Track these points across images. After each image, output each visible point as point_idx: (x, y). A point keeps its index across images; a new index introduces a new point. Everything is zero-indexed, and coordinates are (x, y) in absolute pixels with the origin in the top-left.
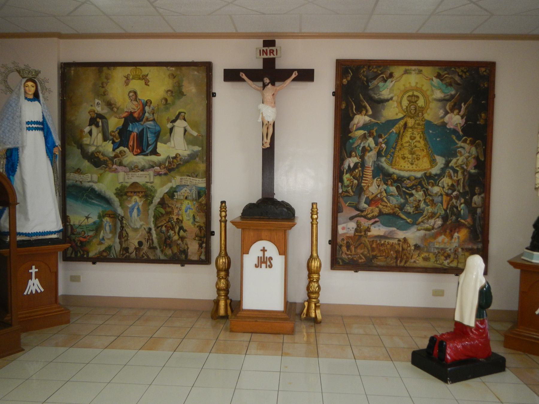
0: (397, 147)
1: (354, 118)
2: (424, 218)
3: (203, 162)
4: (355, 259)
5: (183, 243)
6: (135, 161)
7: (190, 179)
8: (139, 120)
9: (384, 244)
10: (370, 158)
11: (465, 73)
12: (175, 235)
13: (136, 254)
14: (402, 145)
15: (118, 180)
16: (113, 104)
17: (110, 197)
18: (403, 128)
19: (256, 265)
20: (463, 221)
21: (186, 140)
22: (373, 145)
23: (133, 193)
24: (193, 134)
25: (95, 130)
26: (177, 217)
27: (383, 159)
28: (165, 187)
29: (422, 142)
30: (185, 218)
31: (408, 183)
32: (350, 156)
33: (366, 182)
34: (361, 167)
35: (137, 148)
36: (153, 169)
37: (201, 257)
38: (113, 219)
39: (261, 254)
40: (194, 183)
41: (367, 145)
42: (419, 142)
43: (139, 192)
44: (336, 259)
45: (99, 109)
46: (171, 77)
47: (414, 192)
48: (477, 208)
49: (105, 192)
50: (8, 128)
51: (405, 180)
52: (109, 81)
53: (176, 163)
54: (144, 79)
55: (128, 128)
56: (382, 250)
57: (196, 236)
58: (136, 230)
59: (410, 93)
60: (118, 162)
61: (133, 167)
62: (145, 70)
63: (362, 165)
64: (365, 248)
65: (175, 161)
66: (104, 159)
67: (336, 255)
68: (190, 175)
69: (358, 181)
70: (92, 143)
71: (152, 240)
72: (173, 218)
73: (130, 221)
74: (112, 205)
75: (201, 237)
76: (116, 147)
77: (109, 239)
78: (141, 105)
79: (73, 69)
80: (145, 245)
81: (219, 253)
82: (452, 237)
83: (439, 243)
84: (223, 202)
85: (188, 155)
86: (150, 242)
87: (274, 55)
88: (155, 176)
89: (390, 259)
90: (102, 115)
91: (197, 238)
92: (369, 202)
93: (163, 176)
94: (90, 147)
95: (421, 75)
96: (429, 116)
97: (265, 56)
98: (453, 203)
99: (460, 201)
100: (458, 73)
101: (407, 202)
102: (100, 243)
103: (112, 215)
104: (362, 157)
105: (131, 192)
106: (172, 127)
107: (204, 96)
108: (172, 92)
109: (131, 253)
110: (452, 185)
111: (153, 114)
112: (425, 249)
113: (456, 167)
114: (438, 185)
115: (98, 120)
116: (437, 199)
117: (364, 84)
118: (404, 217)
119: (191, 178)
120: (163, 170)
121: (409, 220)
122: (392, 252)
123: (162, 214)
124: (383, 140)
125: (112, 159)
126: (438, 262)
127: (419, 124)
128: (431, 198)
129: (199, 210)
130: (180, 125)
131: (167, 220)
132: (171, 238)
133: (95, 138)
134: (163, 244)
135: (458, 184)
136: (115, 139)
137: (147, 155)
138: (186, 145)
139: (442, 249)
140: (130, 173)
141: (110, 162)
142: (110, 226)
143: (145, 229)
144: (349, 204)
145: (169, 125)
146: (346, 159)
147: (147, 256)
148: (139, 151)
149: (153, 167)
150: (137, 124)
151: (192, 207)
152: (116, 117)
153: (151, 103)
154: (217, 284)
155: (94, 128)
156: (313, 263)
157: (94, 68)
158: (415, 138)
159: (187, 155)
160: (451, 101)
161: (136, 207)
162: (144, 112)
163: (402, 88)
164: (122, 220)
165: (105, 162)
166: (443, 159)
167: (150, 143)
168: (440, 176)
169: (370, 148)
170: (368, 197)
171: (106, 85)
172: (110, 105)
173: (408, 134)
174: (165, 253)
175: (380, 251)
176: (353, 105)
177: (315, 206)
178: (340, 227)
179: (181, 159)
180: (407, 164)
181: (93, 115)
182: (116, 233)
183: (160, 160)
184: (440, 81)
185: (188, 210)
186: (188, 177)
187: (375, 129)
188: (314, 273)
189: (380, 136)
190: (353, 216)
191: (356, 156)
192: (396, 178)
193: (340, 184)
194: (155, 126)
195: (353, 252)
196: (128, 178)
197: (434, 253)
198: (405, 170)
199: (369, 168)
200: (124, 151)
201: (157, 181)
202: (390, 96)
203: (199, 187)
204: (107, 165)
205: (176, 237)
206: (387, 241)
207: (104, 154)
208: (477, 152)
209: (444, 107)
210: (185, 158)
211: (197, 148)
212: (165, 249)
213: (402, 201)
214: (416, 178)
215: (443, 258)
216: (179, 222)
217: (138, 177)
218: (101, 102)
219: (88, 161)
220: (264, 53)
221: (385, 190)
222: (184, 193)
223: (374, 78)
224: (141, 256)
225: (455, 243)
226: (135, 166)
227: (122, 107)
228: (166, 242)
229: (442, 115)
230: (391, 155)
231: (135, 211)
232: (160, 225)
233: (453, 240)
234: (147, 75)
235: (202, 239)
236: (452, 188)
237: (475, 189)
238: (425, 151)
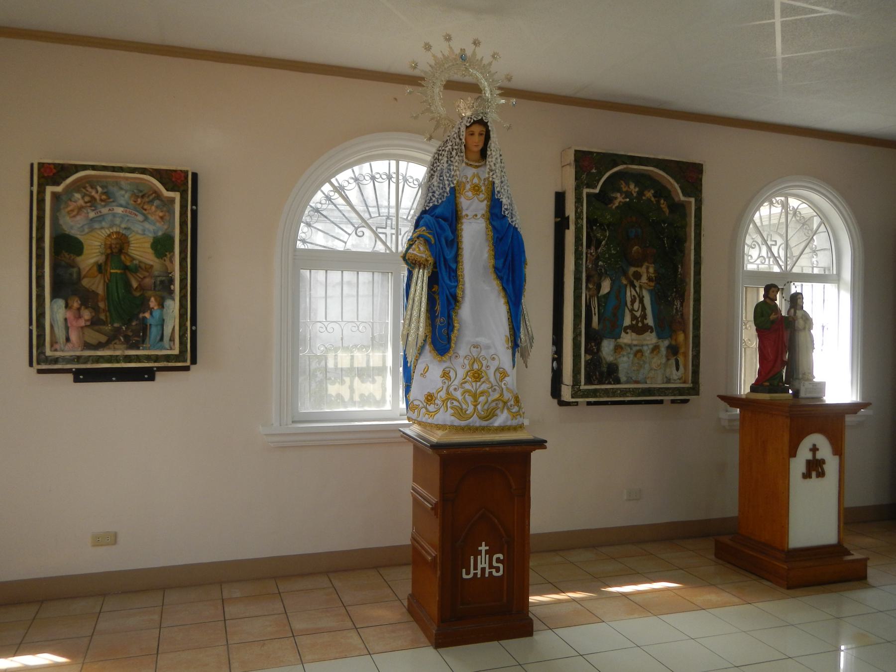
19: (803, 474)
39: (809, 456)
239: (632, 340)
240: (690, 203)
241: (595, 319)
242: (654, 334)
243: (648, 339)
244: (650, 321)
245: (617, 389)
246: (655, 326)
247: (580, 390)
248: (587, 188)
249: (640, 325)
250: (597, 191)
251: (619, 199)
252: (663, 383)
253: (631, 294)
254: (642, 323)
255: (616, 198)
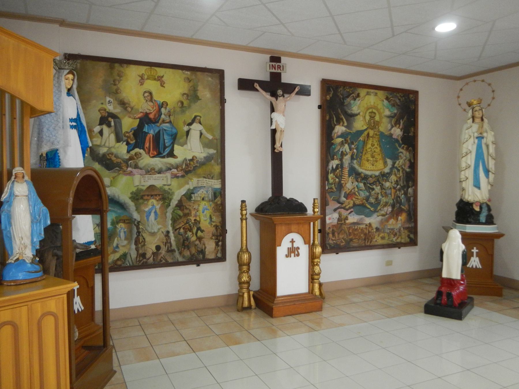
0: (364, 152)
1: (335, 128)
2: (381, 207)
3: (218, 164)
4: (338, 243)
5: (201, 243)
6: (151, 163)
7: (206, 181)
8: (155, 121)
9: (357, 229)
10: (347, 160)
11: (402, 97)
12: (193, 236)
13: (154, 259)
14: (366, 150)
15: (133, 183)
16: (127, 103)
17: (125, 201)
18: (366, 137)
19: (286, 255)
20: (403, 207)
21: (201, 143)
22: (348, 150)
23: (150, 196)
24: (209, 137)
25: (106, 130)
26: (195, 218)
27: (355, 161)
28: (182, 189)
29: (379, 148)
30: (203, 219)
31: (371, 180)
32: (333, 159)
33: (345, 180)
34: (340, 168)
35: (153, 150)
36: (170, 171)
37: (218, 255)
38: (128, 224)
39: (290, 245)
40: (210, 185)
41: (344, 150)
42: (377, 148)
43: (156, 195)
44: (326, 245)
45: (110, 108)
46: (186, 80)
47: (374, 187)
48: (410, 197)
49: (119, 197)
50: (53, 125)
51: (369, 178)
52: (121, 78)
53: (193, 166)
54: (159, 80)
55: (143, 130)
56: (356, 234)
57: (213, 235)
58: (153, 234)
59: (370, 110)
60: (134, 165)
61: (149, 169)
62: (161, 71)
63: (341, 166)
64: (345, 233)
65: (192, 163)
66: (118, 161)
67: (325, 242)
68: (206, 176)
69: (339, 179)
70: (103, 144)
71: (170, 243)
72: (191, 219)
73: (147, 225)
74: (127, 210)
75: (217, 236)
76: (131, 148)
77: (124, 246)
78: (157, 107)
79: (79, 61)
80: (163, 249)
81: (240, 249)
82: (397, 219)
83: (390, 225)
84: (243, 202)
85: (205, 157)
86: (168, 245)
87: (281, 70)
88: (172, 178)
89: (361, 241)
90: (114, 114)
91: (213, 237)
92: (347, 196)
93: (180, 178)
94: (101, 148)
95: (376, 96)
96: (382, 129)
97: (273, 71)
98: (397, 194)
99: (401, 192)
100: (398, 97)
101: (370, 195)
102: (114, 252)
103: (127, 220)
104: (341, 160)
105: (148, 195)
106: (188, 129)
107: (218, 101)
108: (188, 95)
109: (148, 259)
110: (397, 181)
111: (169, 116)
112: (382, 231)
113: (399, 167)
114: (389, 181)
115: (110, 119)
116: (388, 192)
117: (341, 100)
118: (369, 206)
119: (208, 180)
120: (180, 172)
121: (372, 209)
122: (362, 235)
123: (179, 216)
124: (355, 146)
125: (126, 161)
126: (390, 240)
127: (376, 135)
128: (385, 191)
129: (215, 210)
130: (196, 128)
131: (185, 222)
132: (189, 239)
133: (107, 139)
134: (181, 246)
135: (400, 180)
136: (129, 140)
137: (163, 157)
138: (202, 148)
139: (392, 229)
140: (147, 176)
141: (124, 164)
142: (125, 232)
143: (162, 232)
144: (333, 198)
145: (186, 128)
146: (330, 161)
147: (165, 260)
148: (155, 153)
149: (170, 169)
150: (153, 125)
151: (209, 208)
152: (130, 117)
153: (167, 105)
154: (239, 278)
155: (105, 128)
156: (317, 250)
157: (104, 63)
158: (374, 145)
159: (203, 158)
160: (394, 117)
161: (153, 211)
162: (160, 114)
163: (366, 106)
164: (139, 225)
165: (119, 165)
166: (391, 161)
167: (167, 145)
168: (390, 174)
169: (346, 152)
170: (345, 192)
171: (119, 83)
172: (123, 104)
173: (370, 142)
174: (183, 255)
175: (354, 234)
176: (334, 117)
177: (316, 201)
178: (327, 218)
179: (197, 162)
180: (370, 165)
181: (104, 114)
182: (131, 239)
183: (178, 163)
184: (388, 103)
185: (205, 210)
186: (205, 179)
187: (349, 138)
188: (244, 265)
189: (353, 143)
190: (336, 208)
191: (337, 159)
192: (363, 176)
193: (327, 182)
194: (172, 128)
195: (337, 238)
196: (144, 181)
197: (388, 233)
198: (368, 170)
199: (346, 168)
200: (139, 152)
201: (174, 183)
202: (358, 112)
203: (215, 188)
204: (121, 168)
205: (194, 238)
206: (359, 226)
207: (118, 156)
208: (410, 156)
209: (391, 122)
210: (201, 161)
211: (212, 151)
212: (183, 251)
213: (368, 194)
214: (376, 176)
215: (392, 236)
216: (196, 223)
217: (155, 179)
218: (113, 100)
219: (99, 163)
220: (273, 68)
221: (357, 186)
222: (201, 194)
223: (348, 97)
224: (158, 260)
225: (399, 225)
226: (152, 168)
227: (136, 107)
228: (185, 244)
229: (389, 128)
230: (360, 158)
231: (153, 215)
232: (178, 227)
233: (398, 222)
234: (163, 77)
235: (219, 238)
236: (397, 183)
237: (409, 183)
238: (381, 154)
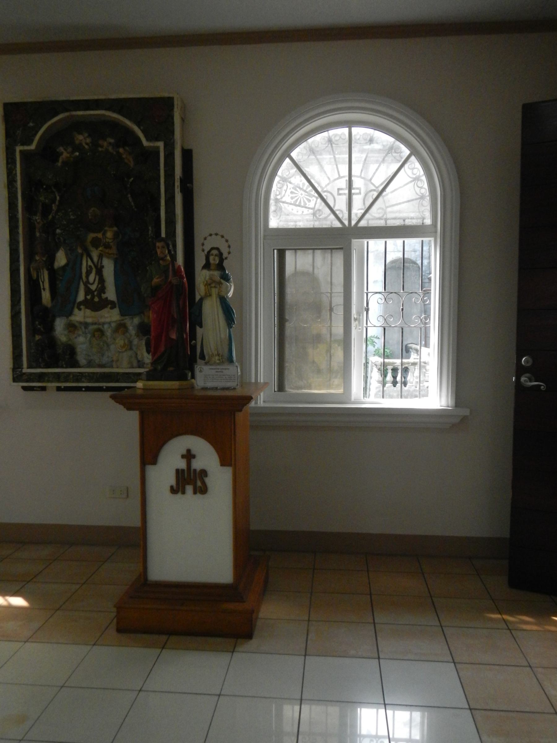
19: (172, 487)
39: (182, 464)
239: (85, 317)
240: (158, 148)
241: (46, 296)
242: (116, 311)
243: (106, 315)
244: (111, 294)
245: (70, 373)
246: (118, 299)
247: (24, 374)
248: (23, 144)
249: (96, 299)
250: (33, 147)
251: (65, 154)
252: (133, 368)
253: (87, 264)
254: (98, 298)
255: (62, 153)
